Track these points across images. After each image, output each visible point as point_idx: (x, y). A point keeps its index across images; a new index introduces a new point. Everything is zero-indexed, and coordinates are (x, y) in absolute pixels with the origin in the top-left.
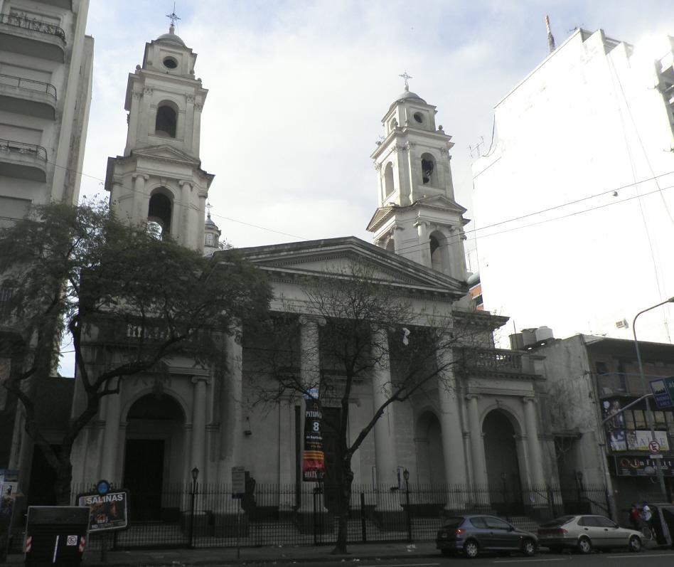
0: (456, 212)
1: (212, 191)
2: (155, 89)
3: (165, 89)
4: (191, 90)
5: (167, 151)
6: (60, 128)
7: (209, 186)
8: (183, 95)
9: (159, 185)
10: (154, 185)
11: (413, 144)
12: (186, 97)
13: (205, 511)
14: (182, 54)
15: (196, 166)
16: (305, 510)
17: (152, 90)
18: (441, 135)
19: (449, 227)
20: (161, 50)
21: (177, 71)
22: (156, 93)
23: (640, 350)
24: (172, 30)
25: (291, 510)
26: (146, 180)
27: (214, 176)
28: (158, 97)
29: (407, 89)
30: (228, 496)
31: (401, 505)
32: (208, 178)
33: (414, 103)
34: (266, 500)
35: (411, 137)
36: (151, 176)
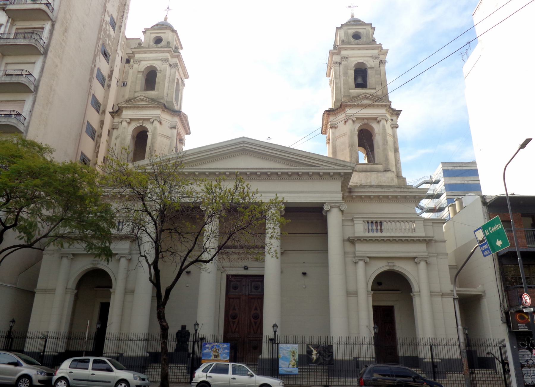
0: (381, 106)
1: (401, 120)
2: (141, 60)
3: (357, 55)
4: (375, 52)
5: (366, 98)
6: (35, 97)
7: (397, 118)
8: (372, 57)
9: (138, 125)
10: (134, 125)
11: (345, 58)
12: (162, 61)
13: (441, 359)
14: (165, 33)
15: (388, 106)
16: (346, 358)
17: (139, 62)
18: (379, 47)
19: (375, 119)
20: (151, 33)
21: (163, 43)
22: (142, 63)
23: (512, 205)
24: (166, 19)
25: (372, 359)
26: (353, 122)
27: (401, 111)
28: (144, 65)
29: (166, 19)
30: (427, 347)
31: (147, 352)
32: (397, 113)
33: (356, 25)
34: (482, 353)
35: (344, 53)
36: (358, 118)
